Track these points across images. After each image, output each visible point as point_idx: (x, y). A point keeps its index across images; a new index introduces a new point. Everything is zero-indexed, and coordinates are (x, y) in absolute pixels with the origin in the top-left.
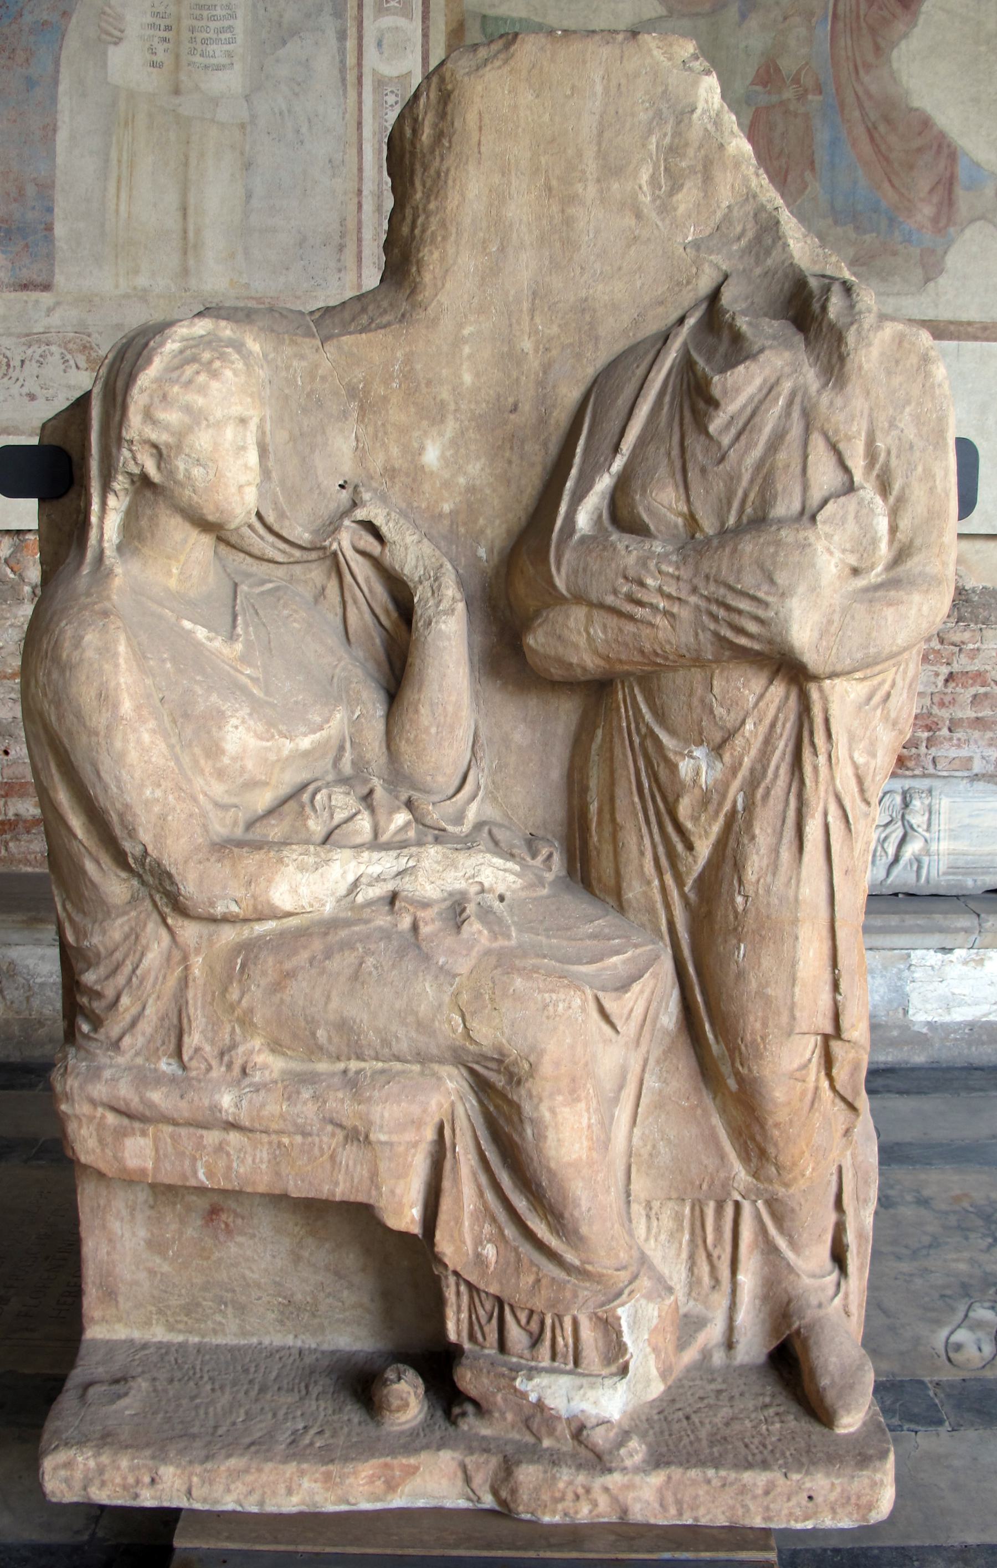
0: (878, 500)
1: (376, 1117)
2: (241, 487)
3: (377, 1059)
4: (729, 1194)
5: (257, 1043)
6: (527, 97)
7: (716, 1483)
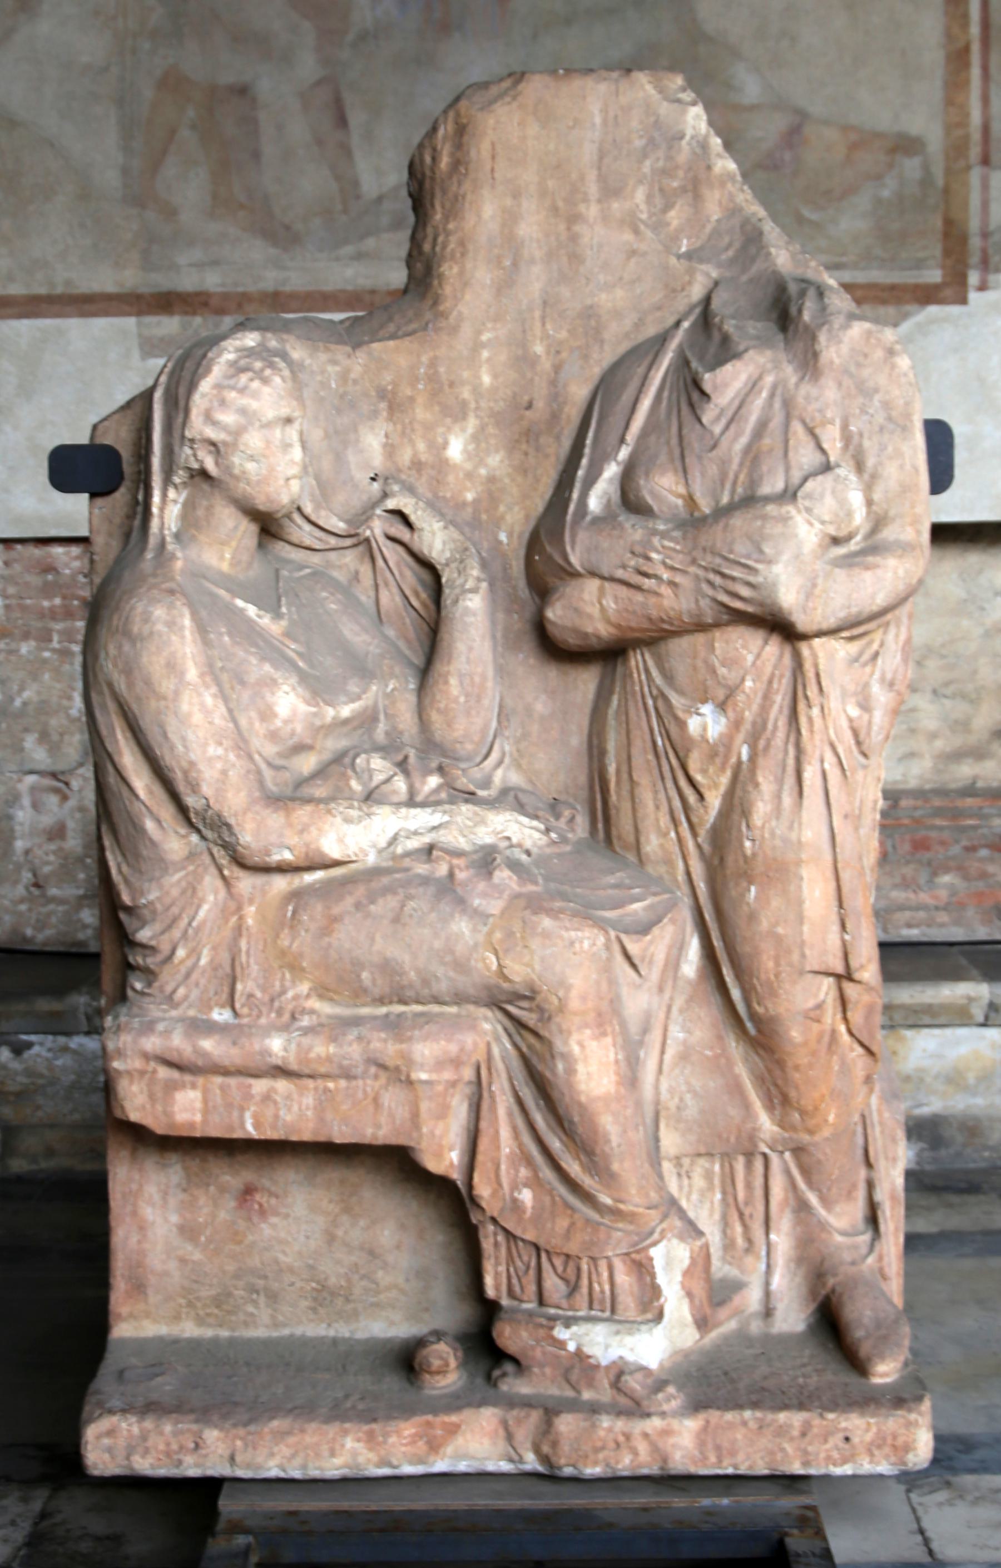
0: (853, 478)
1: (417, 1057)
2: (288, 479)
3: (418, 1002)
4: (756, 1146)
5: (304, 988)
6: (533, 129)
7: (753, 1425)
